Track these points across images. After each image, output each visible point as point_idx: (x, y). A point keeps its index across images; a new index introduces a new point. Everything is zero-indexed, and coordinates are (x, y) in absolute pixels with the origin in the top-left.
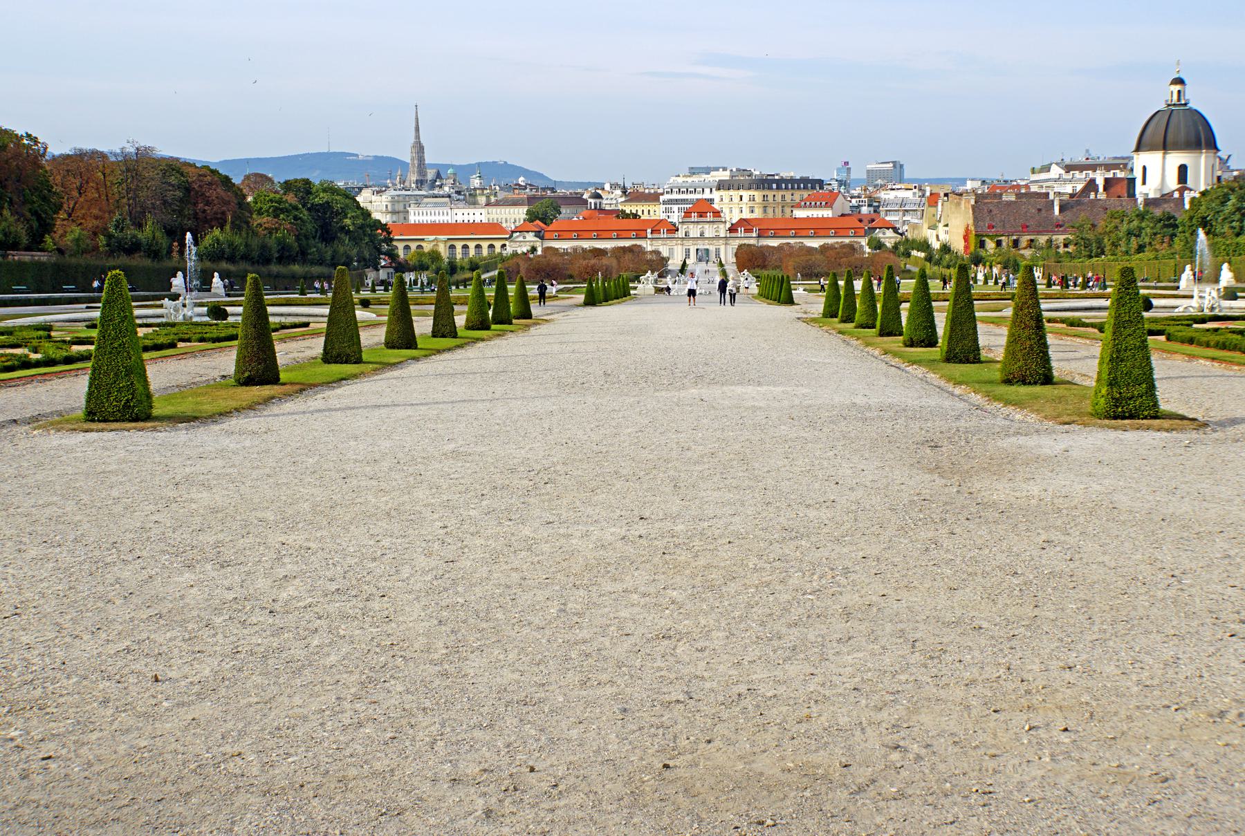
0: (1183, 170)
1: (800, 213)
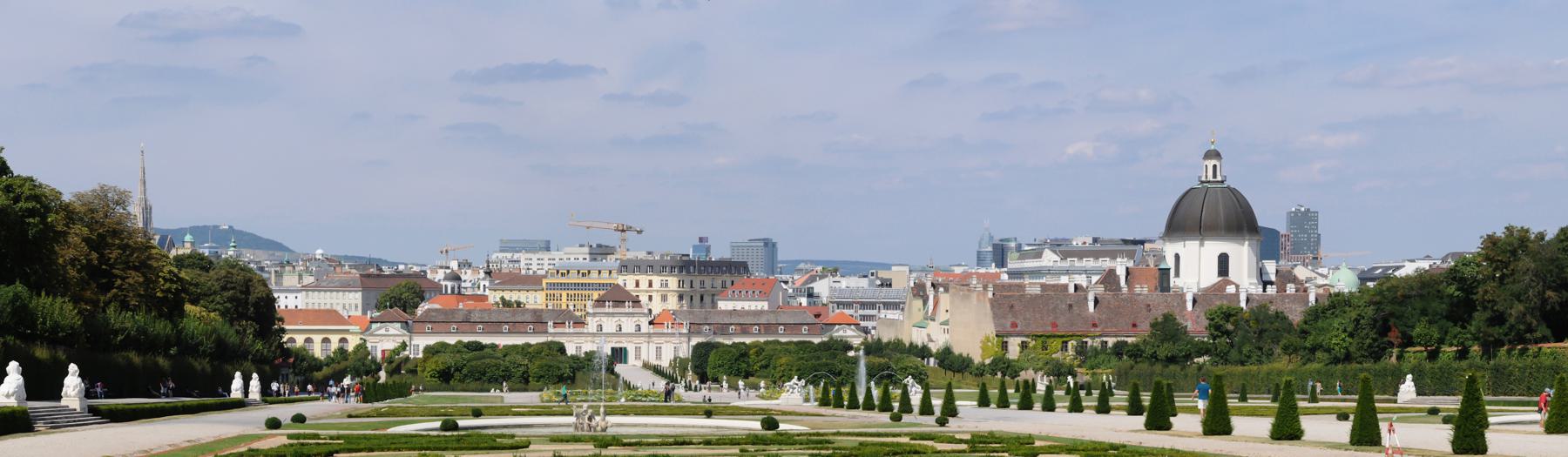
0: (1223, 261)
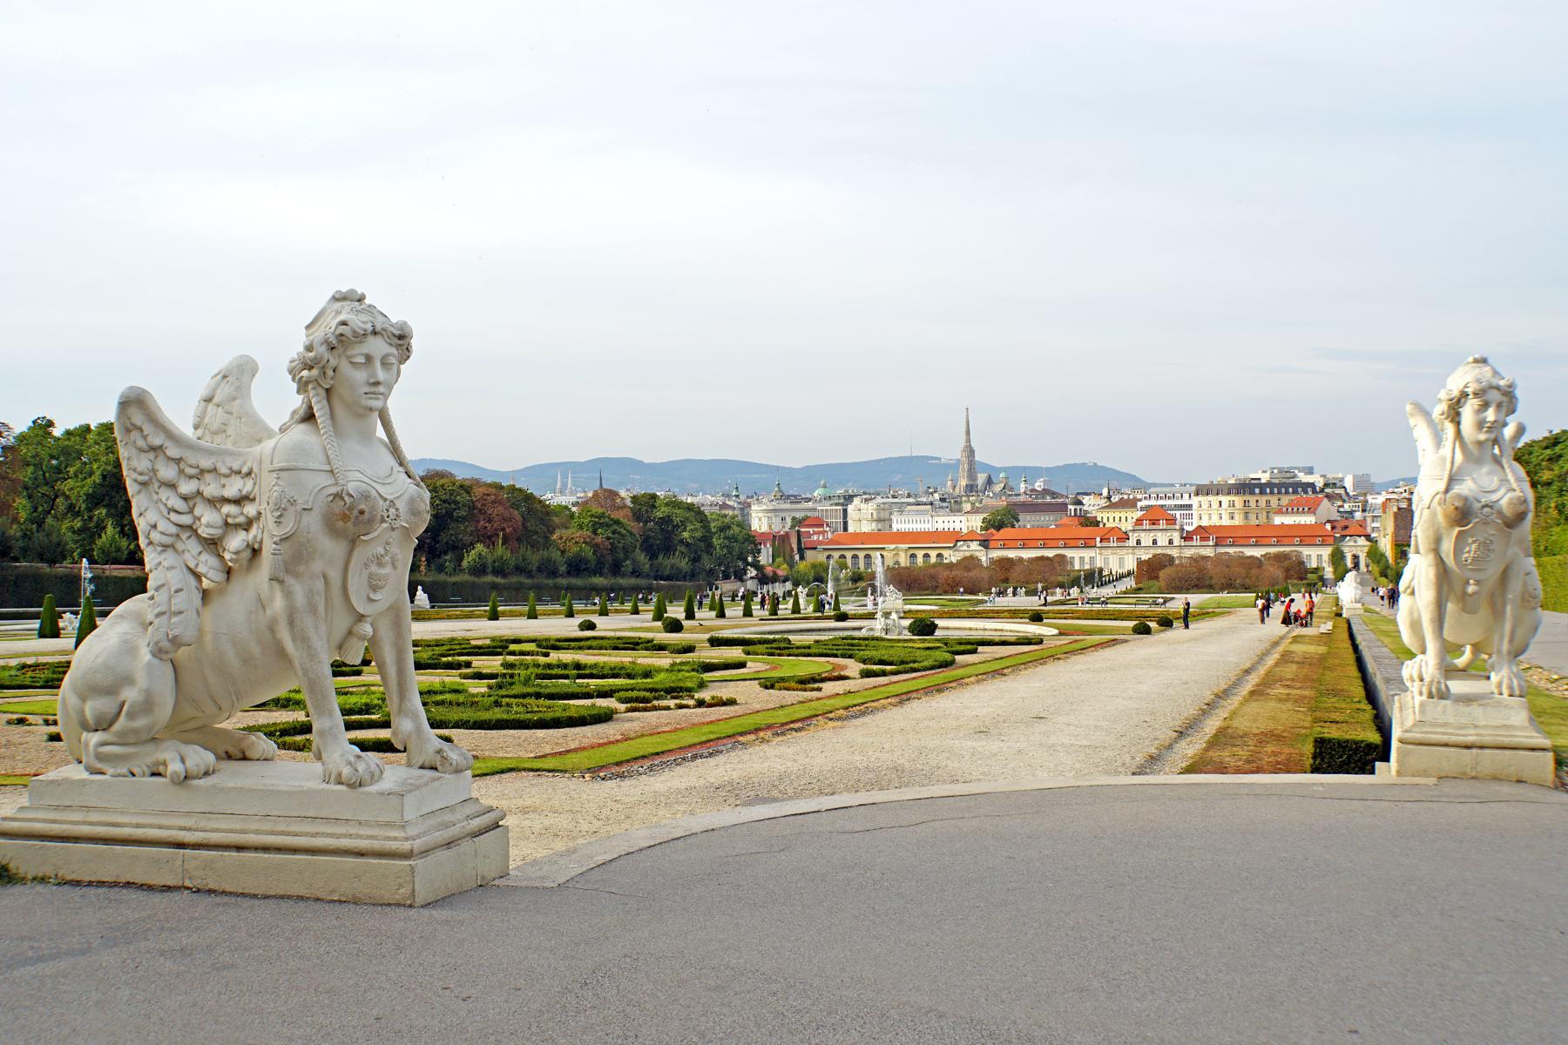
1: (1278, 520)
